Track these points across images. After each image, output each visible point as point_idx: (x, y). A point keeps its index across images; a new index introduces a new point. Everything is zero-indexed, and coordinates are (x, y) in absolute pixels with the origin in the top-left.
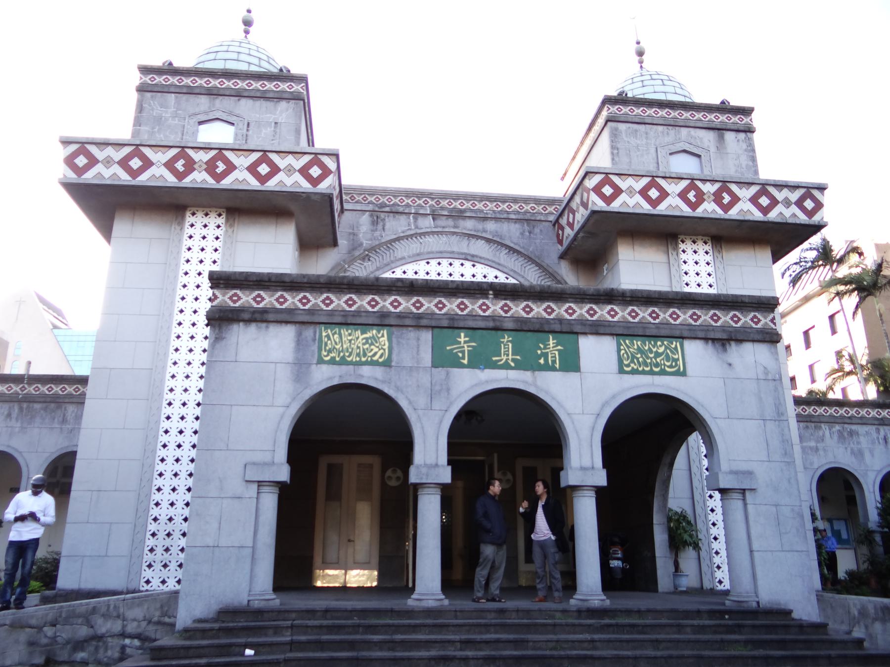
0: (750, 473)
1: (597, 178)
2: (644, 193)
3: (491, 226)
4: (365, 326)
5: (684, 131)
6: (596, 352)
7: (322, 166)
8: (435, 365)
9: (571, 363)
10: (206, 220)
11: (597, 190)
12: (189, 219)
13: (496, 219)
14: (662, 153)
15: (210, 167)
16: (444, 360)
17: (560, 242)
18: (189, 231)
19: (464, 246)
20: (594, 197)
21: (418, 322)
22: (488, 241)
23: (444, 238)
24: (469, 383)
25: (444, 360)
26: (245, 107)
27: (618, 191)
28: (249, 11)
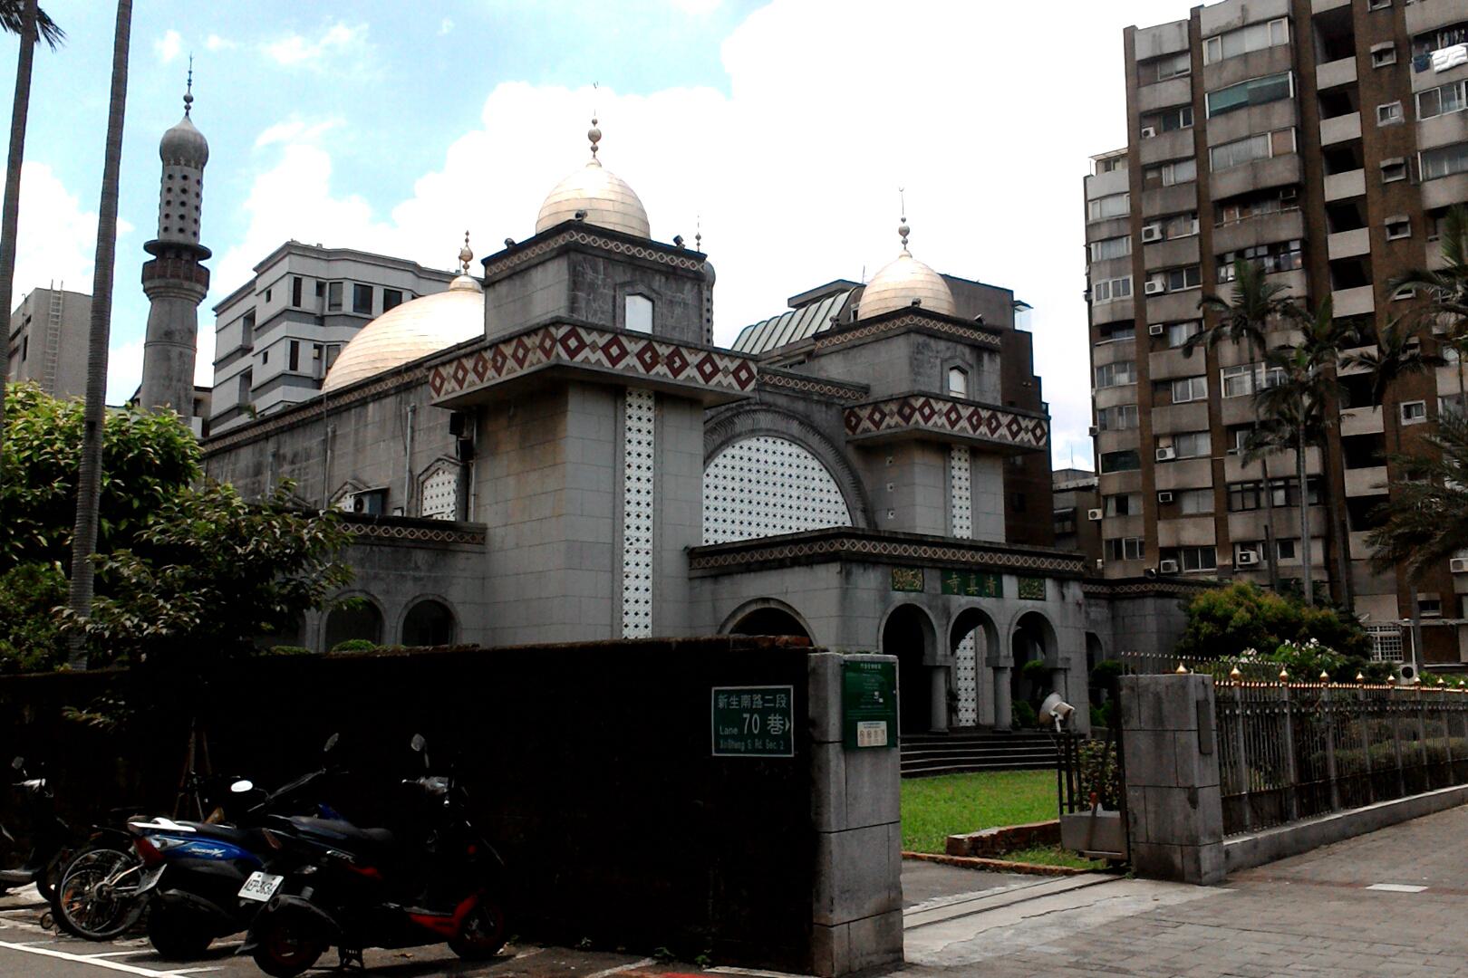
0: (1068, 659)
1: (922, 400)
2: (947, 415)
3: (800, 406)
4: (911, 567)
5: (960, 347)
6: (1010, 585)
7: (749, 371)
8: (944, 592)
9: (999, 594)
10: (640, 402)
11: (921, 410)
12: (629, 399)
13: (804, 399)
14: (946, 367)
15: (670, 364)
16: (947, 590)
17: (853, 429)
18: (629, 411)
19: (781, 424)
20: (917, 416)
21: (934, 563)
22: (801, 423)
23: (770, 416)
24: (960, 602)
25: (947, 590)
26: (658, 282)
27: (933, 412)
28: (595, 123)
